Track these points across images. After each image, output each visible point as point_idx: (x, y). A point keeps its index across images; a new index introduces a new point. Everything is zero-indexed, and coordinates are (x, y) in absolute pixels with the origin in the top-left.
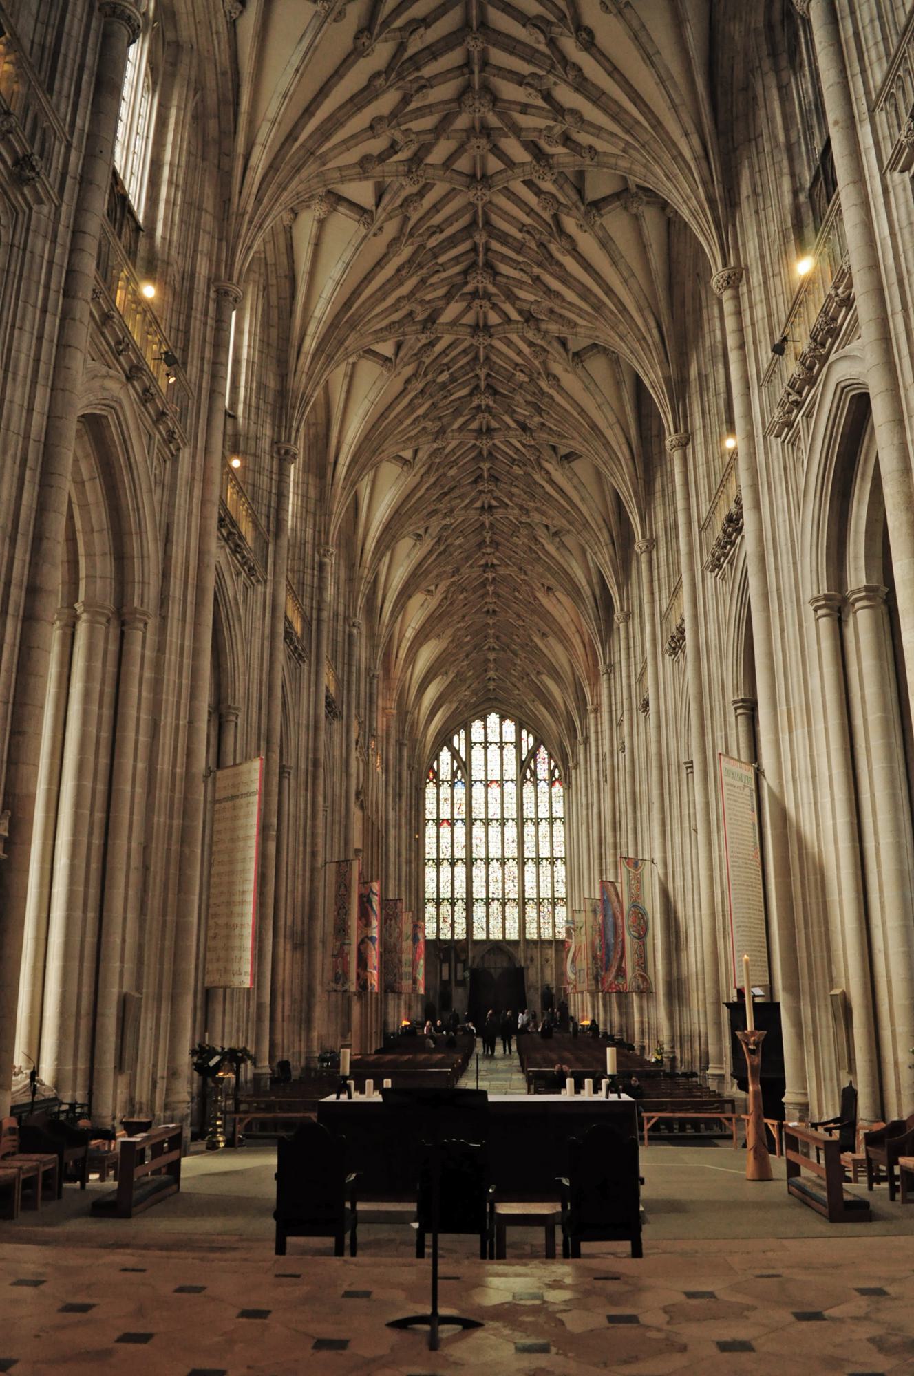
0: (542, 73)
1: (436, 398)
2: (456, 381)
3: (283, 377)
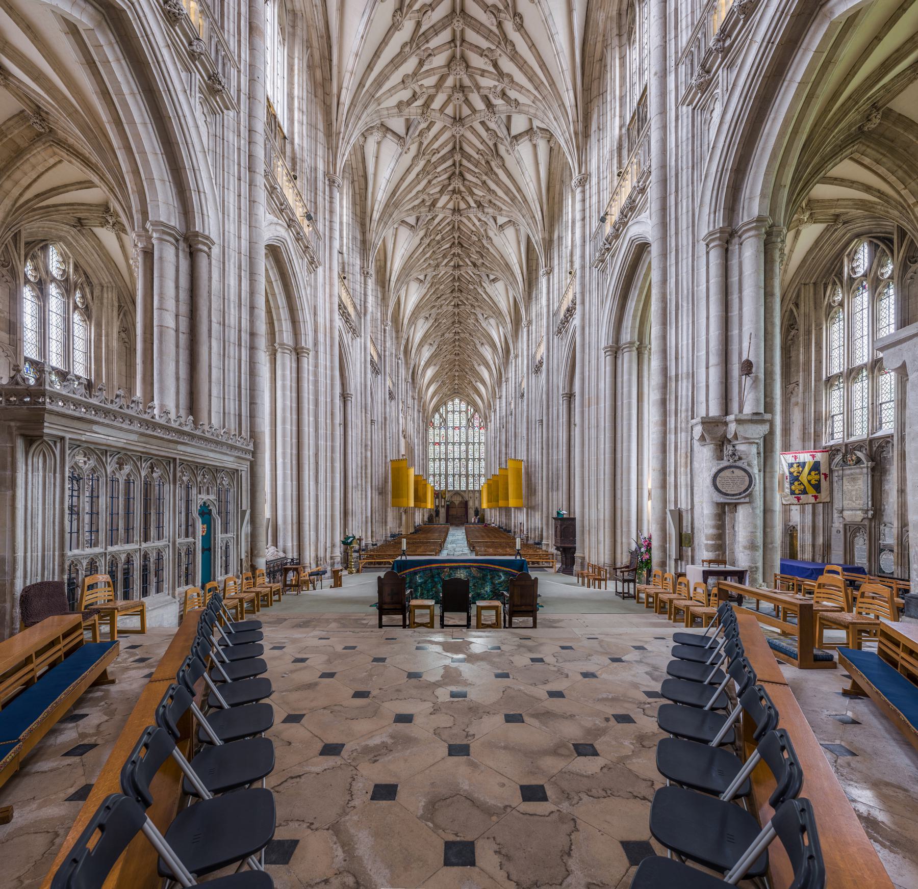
0: (493, 47)
3: (364, 233)
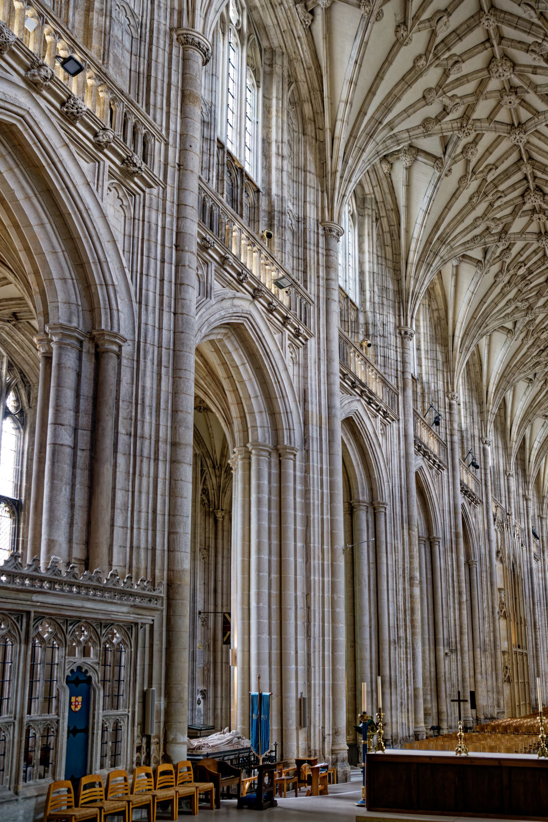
1: (520, 286)
2: (532, 273)
3: (398, 281)
